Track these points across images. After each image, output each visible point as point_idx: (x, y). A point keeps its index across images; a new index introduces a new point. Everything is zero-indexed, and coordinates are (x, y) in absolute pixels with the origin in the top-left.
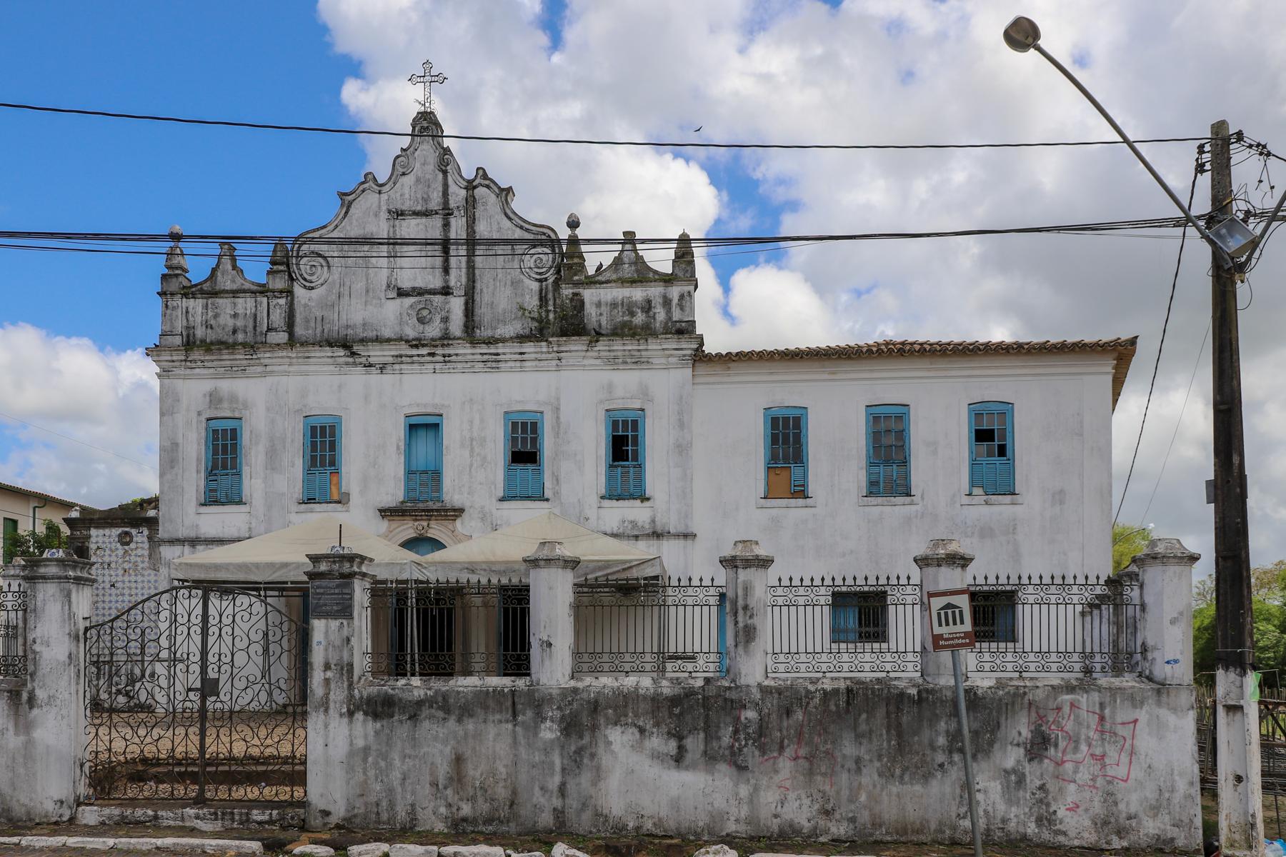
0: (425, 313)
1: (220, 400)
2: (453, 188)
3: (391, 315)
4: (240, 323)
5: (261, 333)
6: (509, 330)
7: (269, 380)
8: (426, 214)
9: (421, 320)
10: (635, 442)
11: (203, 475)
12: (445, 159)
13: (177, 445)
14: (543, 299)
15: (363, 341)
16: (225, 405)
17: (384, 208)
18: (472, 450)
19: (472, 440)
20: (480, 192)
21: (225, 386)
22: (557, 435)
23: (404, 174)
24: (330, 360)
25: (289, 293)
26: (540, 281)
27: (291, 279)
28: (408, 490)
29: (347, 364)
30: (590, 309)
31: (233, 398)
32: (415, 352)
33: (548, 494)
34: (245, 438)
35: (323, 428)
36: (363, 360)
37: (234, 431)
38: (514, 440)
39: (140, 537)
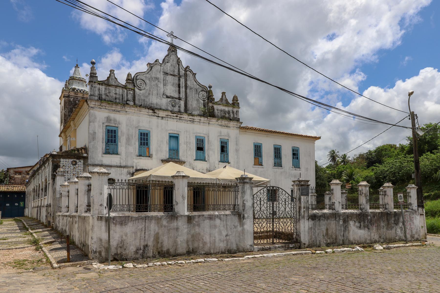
0: (173, 104)
1: (111, 120)
2: (181, 70)
3: (164, 102)
4: (117, 96)
5: (125, 101)
6: (196, 113)
7: (128, 116)
8: (174, 75)
9: (173, 106)
10: (226, 148)
11: (104, 144)
12: (179, 61)
13: (95, 133)
14: (204, 106)
15: (156, 109)
16: (112, 122)
17: (162, 71)
18: (187, 145)
19: (187, 142)
20: (188, 72)
21: (113, 115)
22: (208, 144)
23: (167, 62)
24: (147, 113)
25: (134, 90)
26: (204, 101)
27: (134, 86)
28: (169, 155)
29: (152, 115)
30: (216, 111)
31: (115, 120)
32: (172, 115)
33: (206, 159)
34: (119, 134)
35: (144, 134)
36: (157, 115)
37: (115, 131)
38: (198, 144)
39: (80, 163)
